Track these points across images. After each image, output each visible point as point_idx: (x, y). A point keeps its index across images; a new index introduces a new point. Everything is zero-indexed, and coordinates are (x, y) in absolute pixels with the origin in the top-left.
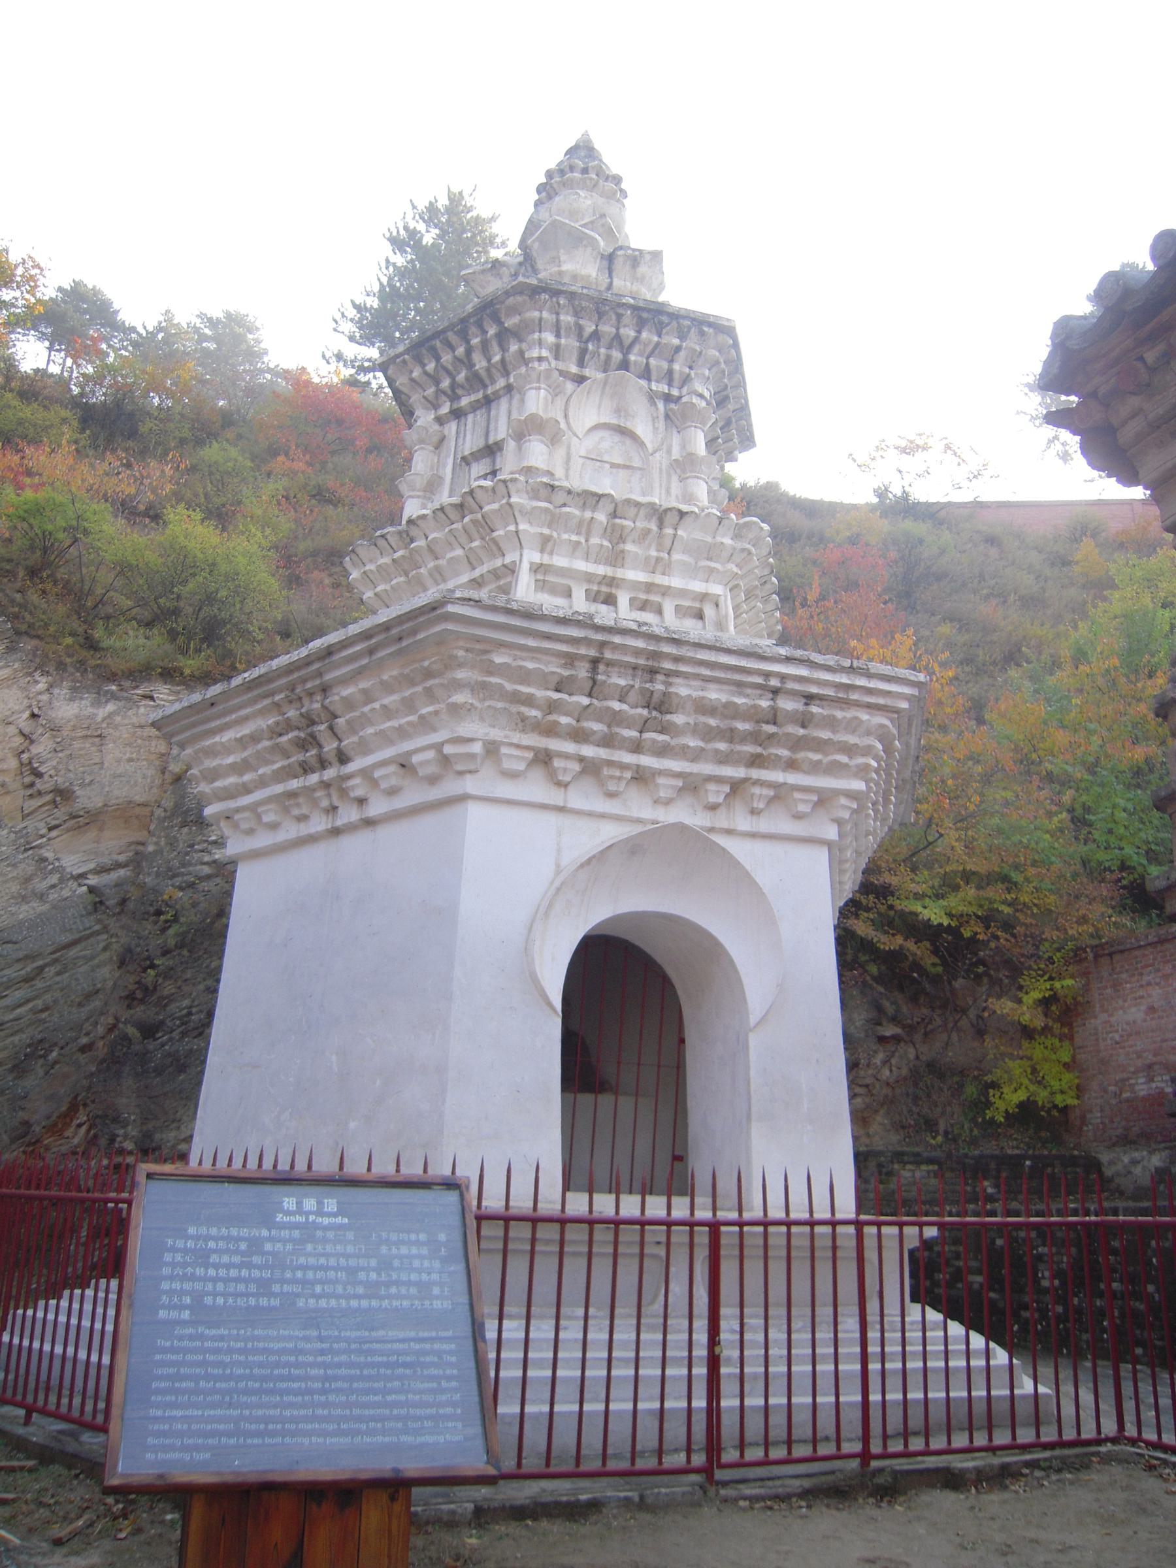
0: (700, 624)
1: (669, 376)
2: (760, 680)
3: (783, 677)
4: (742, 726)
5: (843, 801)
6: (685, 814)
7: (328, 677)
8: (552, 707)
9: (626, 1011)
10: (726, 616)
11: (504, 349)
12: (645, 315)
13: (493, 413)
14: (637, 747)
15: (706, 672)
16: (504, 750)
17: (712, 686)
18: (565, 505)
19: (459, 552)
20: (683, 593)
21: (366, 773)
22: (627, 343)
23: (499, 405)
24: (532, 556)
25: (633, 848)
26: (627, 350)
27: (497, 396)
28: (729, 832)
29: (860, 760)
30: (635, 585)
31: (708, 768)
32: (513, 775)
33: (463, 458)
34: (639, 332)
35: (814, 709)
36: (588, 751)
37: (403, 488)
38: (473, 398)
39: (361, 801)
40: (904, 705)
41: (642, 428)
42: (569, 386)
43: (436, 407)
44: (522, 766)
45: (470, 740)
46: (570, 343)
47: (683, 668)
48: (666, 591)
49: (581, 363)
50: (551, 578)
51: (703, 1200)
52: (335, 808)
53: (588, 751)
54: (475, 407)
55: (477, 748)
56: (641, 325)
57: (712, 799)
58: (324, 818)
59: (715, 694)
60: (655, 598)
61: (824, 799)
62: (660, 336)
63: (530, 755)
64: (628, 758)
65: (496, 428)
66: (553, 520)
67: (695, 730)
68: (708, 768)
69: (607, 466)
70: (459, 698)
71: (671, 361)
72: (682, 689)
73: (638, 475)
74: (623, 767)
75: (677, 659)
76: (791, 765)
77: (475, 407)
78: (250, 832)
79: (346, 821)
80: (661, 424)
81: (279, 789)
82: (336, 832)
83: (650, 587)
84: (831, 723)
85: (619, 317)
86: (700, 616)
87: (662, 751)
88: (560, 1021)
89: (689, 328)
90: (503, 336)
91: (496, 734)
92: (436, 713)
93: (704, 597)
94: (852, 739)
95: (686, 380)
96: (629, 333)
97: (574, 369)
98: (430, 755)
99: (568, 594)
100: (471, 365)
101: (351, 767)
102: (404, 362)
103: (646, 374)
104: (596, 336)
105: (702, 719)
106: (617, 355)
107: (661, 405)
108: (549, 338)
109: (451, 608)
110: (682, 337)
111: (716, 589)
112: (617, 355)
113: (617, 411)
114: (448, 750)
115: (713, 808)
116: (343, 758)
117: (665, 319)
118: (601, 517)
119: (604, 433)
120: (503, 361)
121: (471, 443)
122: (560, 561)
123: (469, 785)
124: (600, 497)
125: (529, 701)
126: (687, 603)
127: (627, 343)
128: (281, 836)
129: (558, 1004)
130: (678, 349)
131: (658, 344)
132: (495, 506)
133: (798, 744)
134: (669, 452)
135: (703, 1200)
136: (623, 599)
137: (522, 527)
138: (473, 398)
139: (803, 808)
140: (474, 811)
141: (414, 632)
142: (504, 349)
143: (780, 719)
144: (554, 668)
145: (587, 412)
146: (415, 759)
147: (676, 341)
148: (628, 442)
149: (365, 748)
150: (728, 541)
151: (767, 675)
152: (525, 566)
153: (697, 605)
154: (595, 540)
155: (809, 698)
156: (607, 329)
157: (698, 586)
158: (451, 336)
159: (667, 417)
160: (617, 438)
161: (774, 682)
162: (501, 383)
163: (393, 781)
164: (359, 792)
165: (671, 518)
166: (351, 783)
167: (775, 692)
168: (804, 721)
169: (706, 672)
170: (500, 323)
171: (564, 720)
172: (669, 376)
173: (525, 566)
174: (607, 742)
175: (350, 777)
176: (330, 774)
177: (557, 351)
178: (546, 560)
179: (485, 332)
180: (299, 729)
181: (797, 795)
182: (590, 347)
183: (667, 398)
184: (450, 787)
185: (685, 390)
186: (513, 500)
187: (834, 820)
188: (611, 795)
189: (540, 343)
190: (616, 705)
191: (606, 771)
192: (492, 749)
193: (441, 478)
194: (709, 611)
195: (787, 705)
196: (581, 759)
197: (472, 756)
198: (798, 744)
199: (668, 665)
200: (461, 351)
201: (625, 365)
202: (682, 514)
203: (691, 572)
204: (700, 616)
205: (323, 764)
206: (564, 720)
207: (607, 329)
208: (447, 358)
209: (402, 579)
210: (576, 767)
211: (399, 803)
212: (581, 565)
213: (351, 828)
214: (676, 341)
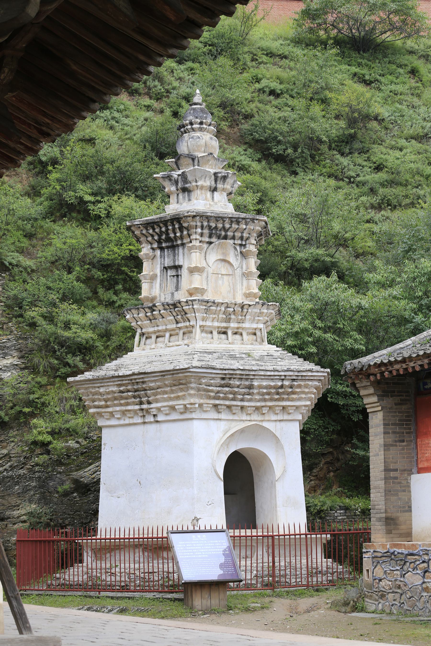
0: (254, 337)
1: (242, 238)
2: (278, 377)
3: (285, 376)
4: (273, 391)
5: (303, 408)
6: (256, 417)
7: (146, 380)
8: (218, 392)
9: (241, 477)
10: (265, 336)
11: (182, 232)
12: (233, 220)
13: (177, 252)
14: (242, 400)
15: (263, 377)
16: (204, 405)
17: (264, 380)
18: (211, 306)
19: (172, 318)
20: (249, 328)
21: (159, 409)
22: (227, 228)
23: (178, 249)
24: (200, 323)
25: (242, 431)
26: (226, 230)
27: (178, 246)
28: (268, 421)
29: (309, 395)
30: (234, 328)
31: (263, 404)
32: (206, 411)
33: (165, 267)
34: (231, 225)
35: (295, 383)
36: (227, 403)
37: (141, 278)
38: (167, 244)
39: (154, 416)
40: (323, 378)
41: (232, 259)
42: (205, 246)
43: (151, 244)
44: (209, 409)
45: (195, 404)
46: (206, 231)
47: (256, 377)
48: (243, 329)
49: (210, 236)
50: (205, 329)
51: (260, 530)
52: (144, 416)
53: (227, 403)
54: (168, 247)
55: (197, 406)
56: (232, 222)
57: (264, 412)
58: (140, 418)
59: (265, 383)
60: (240, 330)
61: (297, 407)
62: (238, 225)
63: (211, 406)
64: (239, 403)
65: (178, 259)
66: (207, 311)
67: (259, 393)
68: (263, 404)
69: (220, 275)
70: (192, 392)
71: (242, 233)
72: (256, 383)
73: (231, 277)
74: (238, 406)
75: (254, 375)
76: (288, 400)
77: (168, 247)
78: (108, 419)
79: (149, 420)
80: (239, 257)
81: (124, 408)
82: (144, 423)
83: (238, 328)
84: (299, 386)
85: (224, 221)
86: (255, 334)
87: (250, 400)
88: (222, 483)
89: (249, 222)
90: (181, 229)
91: (202, 401)
92: (184, 395)
93: (255, 329)
94: (307, 390)
95: (248, 239)
96: (227, 226)
97: (207, 240)
98: (182, 406)
99: (211, 333)
100: (167, 234)
101: (152, 406)
102: (139, 227)
103: (233, 238)
104: (216, 228)
105: (261, 390)
106: (223, 233)
107: (238, 248)
108: (199, 230)
109: (191, 370)
110: (246, 224)
111: (261, 326)
112: (223, 233)
113: (223, 253)
114: (187, 406)
115: (264, 414)
116: (149, 403)
117: (240, 220)
118: (223, 309)
119: (218, 262)
120: (181, 236)
121: (168, 262)
122: (208, 323)
123: (194, 415)
124: (222, 303)
125: (212, 391)
126: (251, 331)
127: (227, 228)
128: (122, 422)
129: (222, 478)
130: (245, 229)
131: (238, 228)
132: (187, 307)
133: (288, 394)
134: (242, 268)
135: (260, 530)
136: (230, 333)
137: (197, 314)
138: (167, 244)
139: (290, 411)
140: (195, 422)
141: (178, 373)
142: (182, 232)
143: (284, 386)
144: (218, 381)
145: (213, 256)
146: (176, 407)
147: (244, 227)
148: (227, 264)
149: (157, 401)
150: (265, 311)
151: (281, 376)
152: (198, 326)
153: (254, 331)
154: (221, 316)
155: (293, 380)
156: (220, 225)
157: (255, 326)
158: (161, 225)
159: (241, 252)
160: (223, 263)
161: (283, 377)
162: (179, 242)
163: (168, 412)
164: (155, 413)
165: (246, 307)
166: (151, 410)
167: (283, 380)
168: (291, 387)
169: (263, 377)
170: (180, 224)
171: (221, 395)
172: (242, 238)
173: (198, 326)
174: (234, 399)
175: (151, 408)
176: (145, 406)
177: (202, 235)
178: (204, 323)
179: (173, 225)
180: (132, 392)
181: (289, 408)
182: (214, 232)
183: (241, 245)
184: (187, 416)
185: (247, 242)
186: (195, 307)
187: (301, 413)
188: (234, 414)
189: (196, 233)
190: (236, 390)
191: (233, 408)
192: (201, 405)
193: (156, 276)
194: (258, 333)
195: (286, 383)
196: (225, 405)
197: (196, 408)
198: (288, 394)
199: (252, 377)
200: (163, 229)
201: (225, 238)
202: (250, 305)
203: (253, 321)
204: (255, 334)
205: (141, 403)
206: (221, 395)
207: (220, 225)
208: (157, 230)
209: (149, 322)
210: (225, 407)
211: (169, 418)
212: (216, 324)
213: (151, 423)
214: (244, 227)
